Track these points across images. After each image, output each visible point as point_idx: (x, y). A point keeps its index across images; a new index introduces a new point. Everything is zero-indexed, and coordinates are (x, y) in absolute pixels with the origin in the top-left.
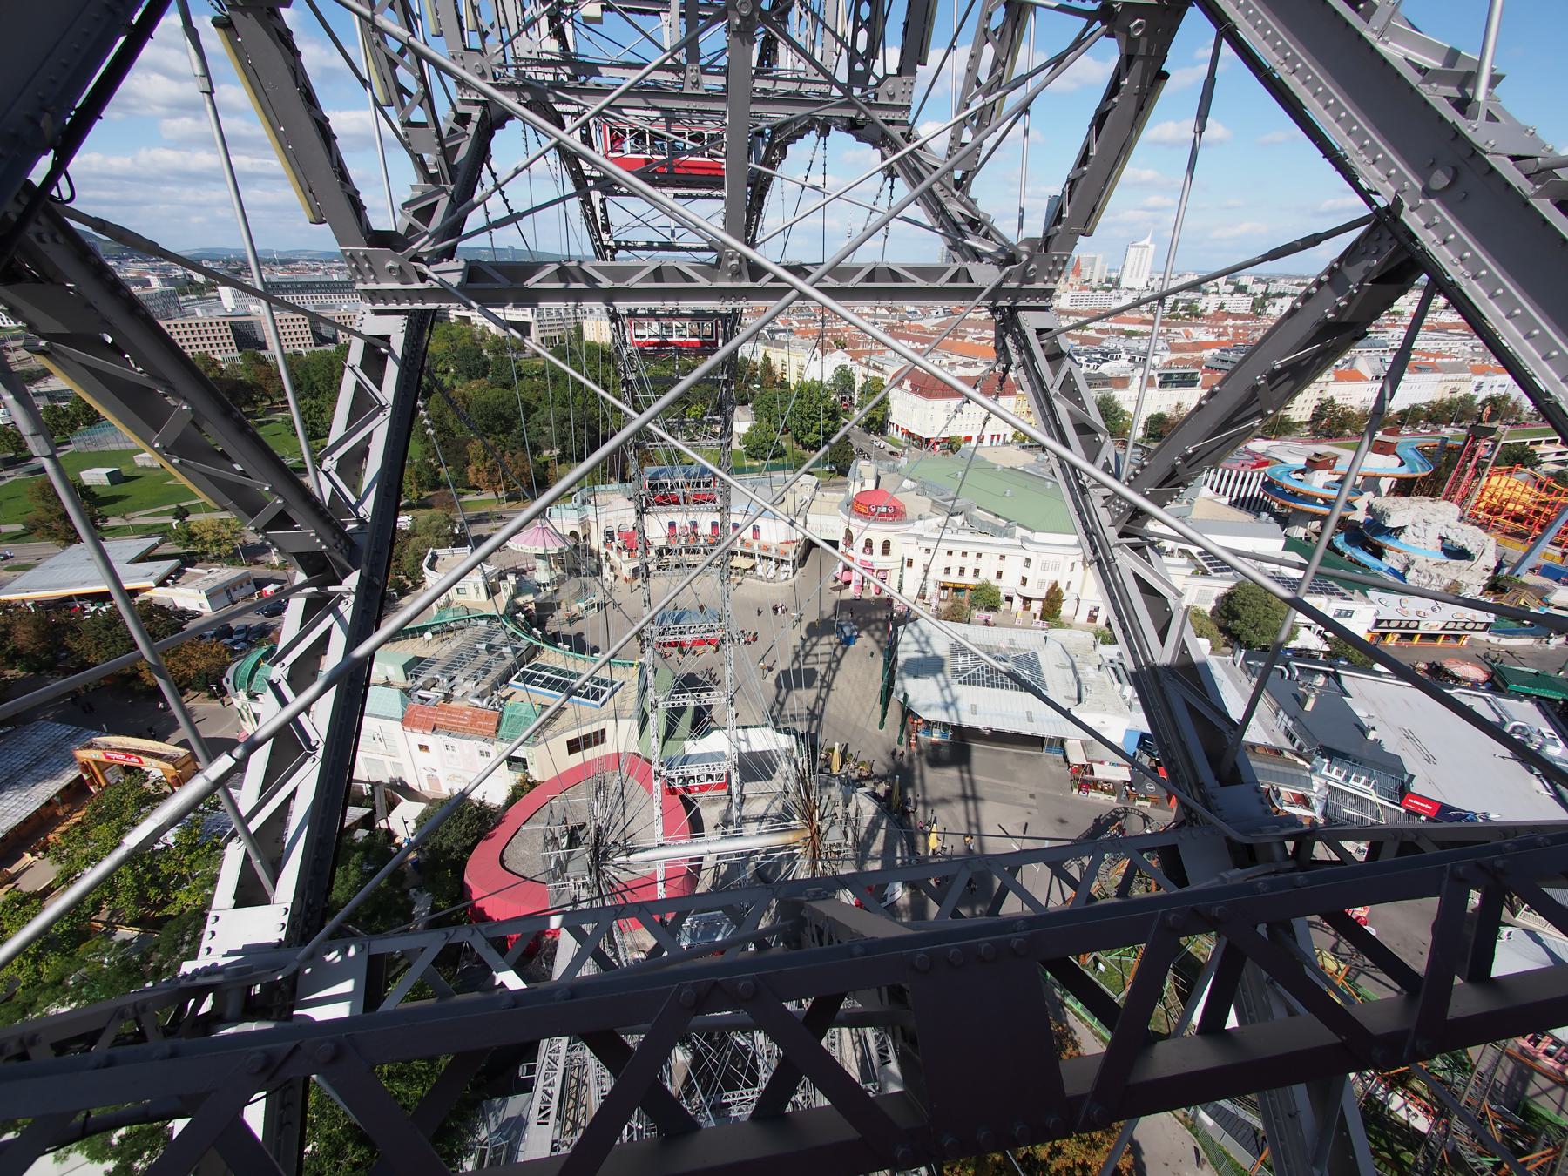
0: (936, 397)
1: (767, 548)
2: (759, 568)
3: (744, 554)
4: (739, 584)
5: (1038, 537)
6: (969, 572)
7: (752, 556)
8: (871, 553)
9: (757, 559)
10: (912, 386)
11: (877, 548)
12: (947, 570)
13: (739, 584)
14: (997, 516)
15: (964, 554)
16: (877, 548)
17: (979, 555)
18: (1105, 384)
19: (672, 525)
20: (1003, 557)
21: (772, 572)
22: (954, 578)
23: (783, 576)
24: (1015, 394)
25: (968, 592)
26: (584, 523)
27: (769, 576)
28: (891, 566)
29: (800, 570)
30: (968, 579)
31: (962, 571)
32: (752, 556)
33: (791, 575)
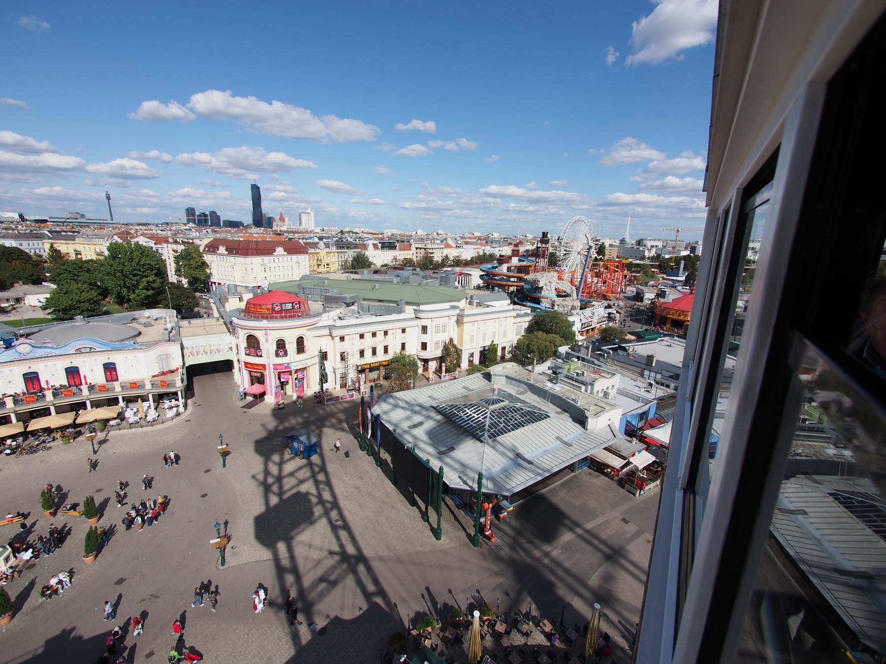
0: (252, 254)
1: (134, 385)
2: (129, 414)
3: (97, 404)
4: (102, 442)
5: (422, 307)
6: (380, 351)
7: (113, 401)
8: (286, 354)
9: (122, 403)
10: (226, 250)
11: (291, 347)
12: (362, 353)
13: (102, 442)
14: (380, 301)
15: (374, 335)
16: (291, 347)
17: (386, 333)
18: (356, 248)
20: (404, 331)
21: (152, 415)
22: (369, 359)
23: (170, 414)
24: (307, 253)
25: (382, 368)
27: (149, 418)
28: (309, 362)
29: (190, 401)
30: (381, 357)
31: (374, 352)
32: (113, 401)
33: (181, 409)
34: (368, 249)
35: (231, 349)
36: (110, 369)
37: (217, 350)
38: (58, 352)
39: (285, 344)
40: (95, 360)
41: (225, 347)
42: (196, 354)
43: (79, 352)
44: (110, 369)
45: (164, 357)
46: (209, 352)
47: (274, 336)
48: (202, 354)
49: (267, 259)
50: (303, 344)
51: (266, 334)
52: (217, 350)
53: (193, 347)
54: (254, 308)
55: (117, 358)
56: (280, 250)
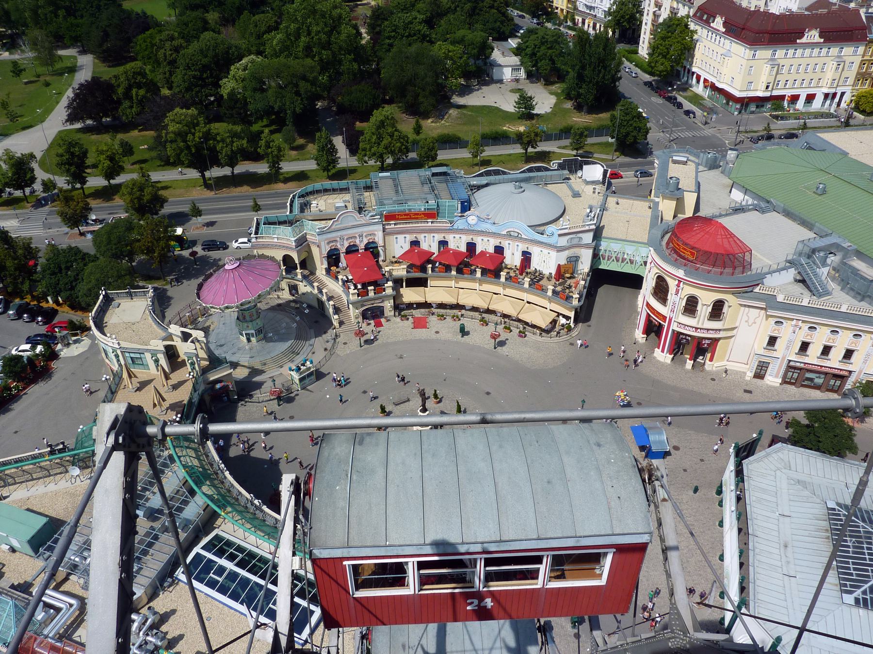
10: (725, 24)
16: (704, 310)
19: (415, 243)
26: (302, 242)
35: (645, 263)
36: (527, 257)
37: (630, 260)
38: (493, 229)
39: (697, 303)
40: (518, 246)
41: (639, 259)
42: (606, 259)
43: (509, 235)
44: (527, 257)
45: (574, 259)
46: (620, 261)
47: (688, 291)
48: (613, 260)
49: (780, 53)
50: (722, 310)
51: (678, 286)
52: (630, 260)
53: (606, 250)
54: (678, 245)
55: (535, 251)
56: (813, 36)
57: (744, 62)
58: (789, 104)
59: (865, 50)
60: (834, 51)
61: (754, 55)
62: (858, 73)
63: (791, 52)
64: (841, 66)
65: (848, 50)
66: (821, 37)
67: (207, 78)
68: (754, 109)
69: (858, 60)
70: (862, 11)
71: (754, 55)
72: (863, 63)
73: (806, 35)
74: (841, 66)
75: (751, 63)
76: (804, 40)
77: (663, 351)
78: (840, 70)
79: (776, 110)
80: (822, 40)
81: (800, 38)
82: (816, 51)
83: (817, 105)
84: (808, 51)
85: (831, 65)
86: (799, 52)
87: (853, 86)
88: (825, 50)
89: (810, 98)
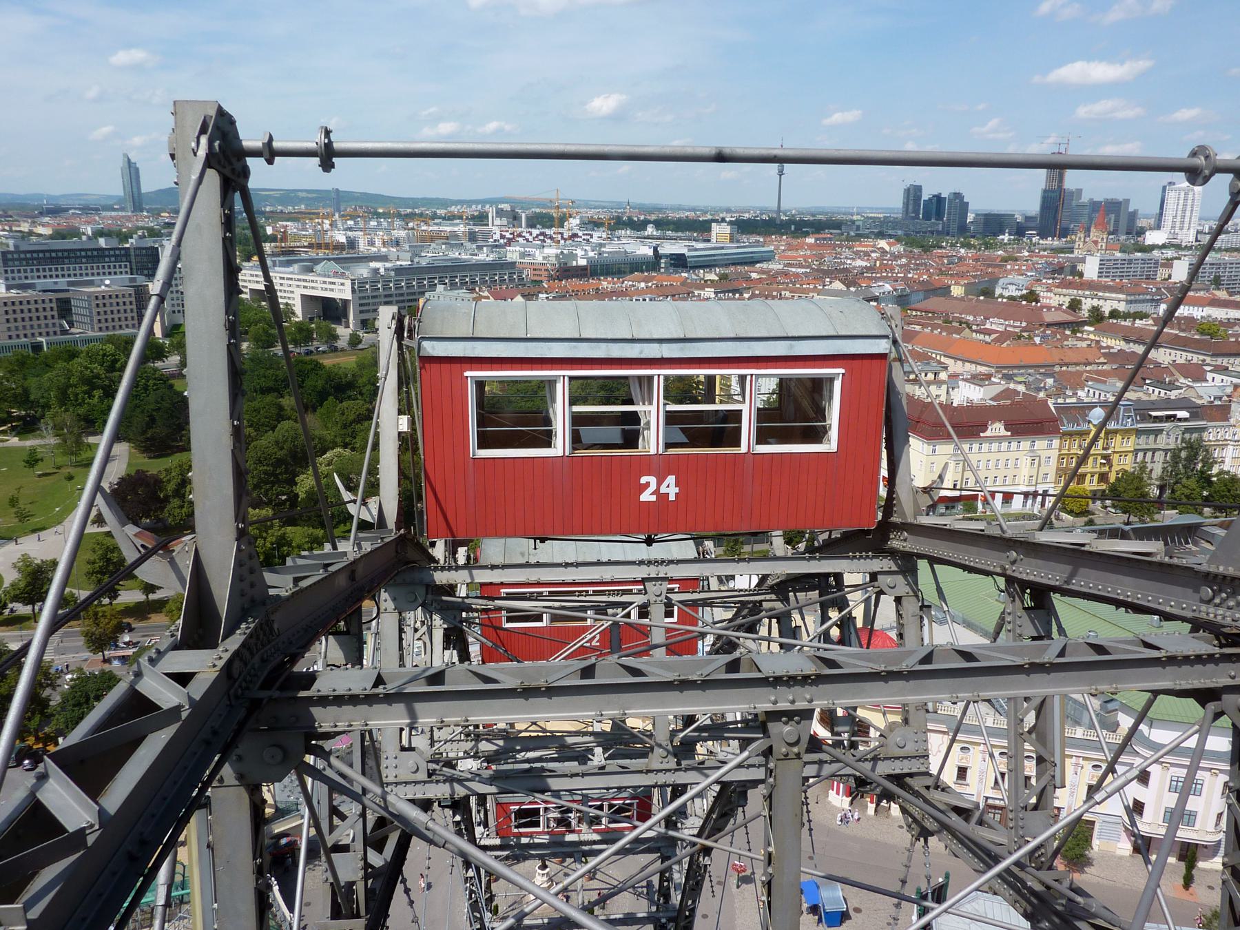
34: (1232, 421)
57: (924, 458)
58: (983, 505)
59: (1061, 443)
60: (1025, 444)
61: (934, 451)
62: (1058, 469)
63: (976, 446)
64: (1036, 462)
65: (1041, 444)
66: (1006, 429)
67: (281, 474)
68: (943, 511)
69: (1054, 454)
70: (1050, 402)
71: (934, 451)
72: (1061, 458)
73: (990, 428)
74: (1036, 462)
75: (933, 459)
76: (988, 433)
77: (838, 793)
78: (1036, 465)
79: (969, 512)
80: (1009, 433)
81: (983, 432)
82: (1004, 445)
83: (1017, 502)
84: (995, 446)
85: (1025, 461)
86: (985, 446)
87: (1055, 483)
88: (1014, 445)
89: (1008, 497)
